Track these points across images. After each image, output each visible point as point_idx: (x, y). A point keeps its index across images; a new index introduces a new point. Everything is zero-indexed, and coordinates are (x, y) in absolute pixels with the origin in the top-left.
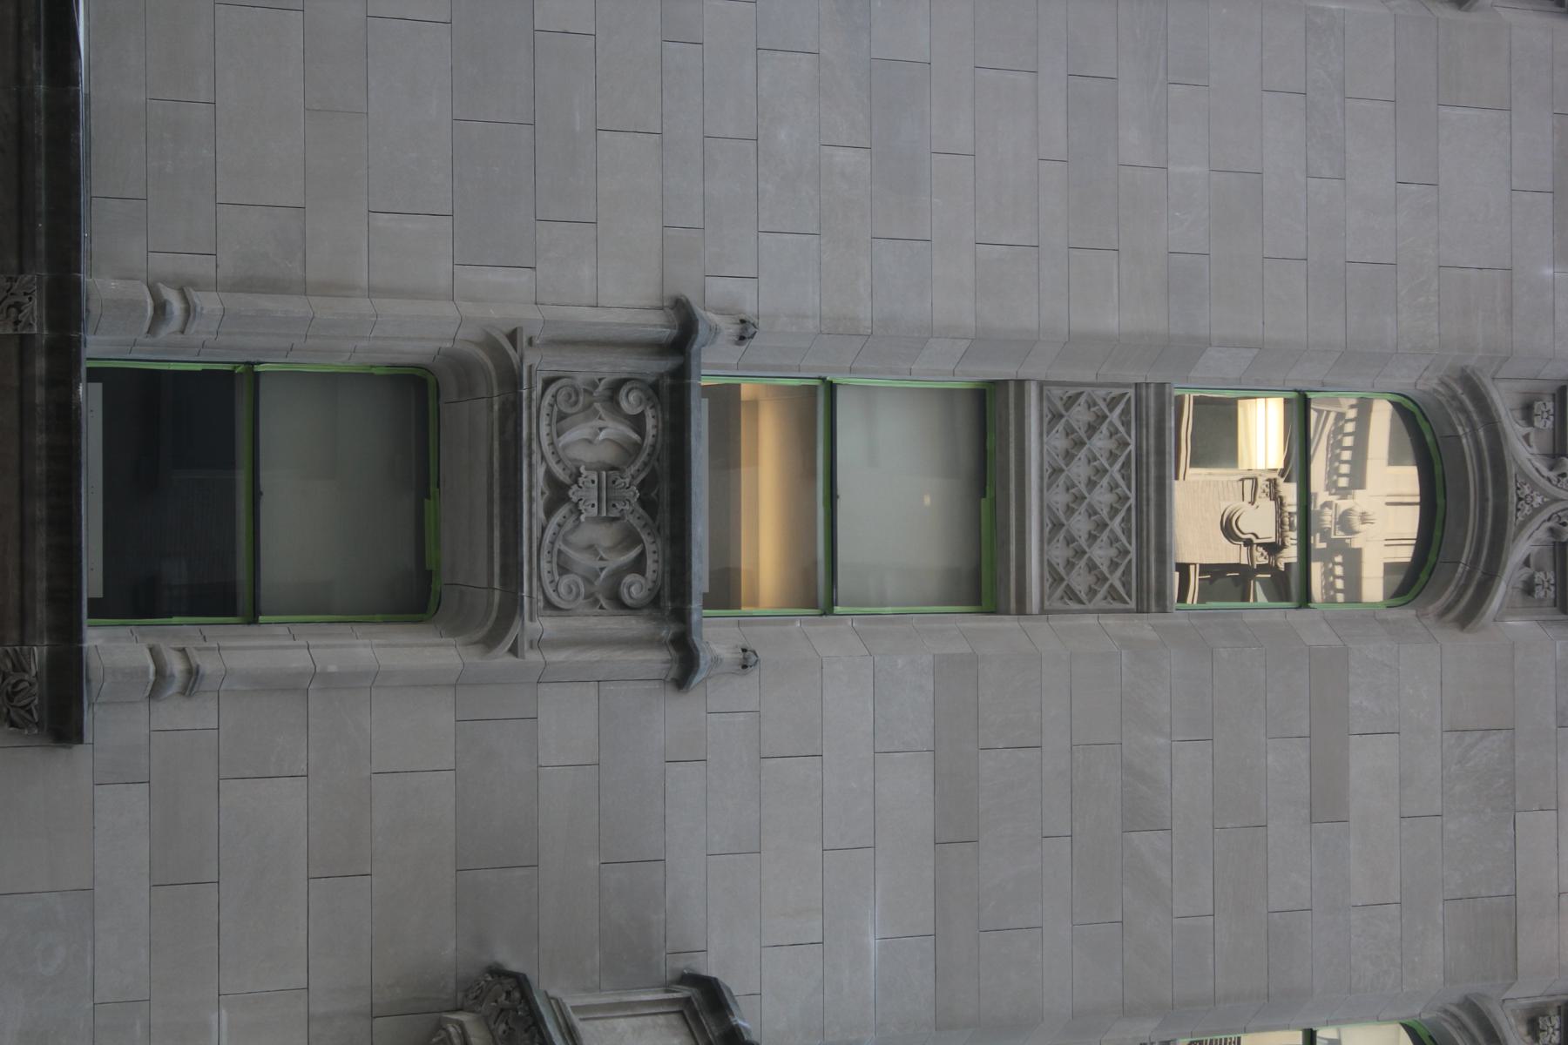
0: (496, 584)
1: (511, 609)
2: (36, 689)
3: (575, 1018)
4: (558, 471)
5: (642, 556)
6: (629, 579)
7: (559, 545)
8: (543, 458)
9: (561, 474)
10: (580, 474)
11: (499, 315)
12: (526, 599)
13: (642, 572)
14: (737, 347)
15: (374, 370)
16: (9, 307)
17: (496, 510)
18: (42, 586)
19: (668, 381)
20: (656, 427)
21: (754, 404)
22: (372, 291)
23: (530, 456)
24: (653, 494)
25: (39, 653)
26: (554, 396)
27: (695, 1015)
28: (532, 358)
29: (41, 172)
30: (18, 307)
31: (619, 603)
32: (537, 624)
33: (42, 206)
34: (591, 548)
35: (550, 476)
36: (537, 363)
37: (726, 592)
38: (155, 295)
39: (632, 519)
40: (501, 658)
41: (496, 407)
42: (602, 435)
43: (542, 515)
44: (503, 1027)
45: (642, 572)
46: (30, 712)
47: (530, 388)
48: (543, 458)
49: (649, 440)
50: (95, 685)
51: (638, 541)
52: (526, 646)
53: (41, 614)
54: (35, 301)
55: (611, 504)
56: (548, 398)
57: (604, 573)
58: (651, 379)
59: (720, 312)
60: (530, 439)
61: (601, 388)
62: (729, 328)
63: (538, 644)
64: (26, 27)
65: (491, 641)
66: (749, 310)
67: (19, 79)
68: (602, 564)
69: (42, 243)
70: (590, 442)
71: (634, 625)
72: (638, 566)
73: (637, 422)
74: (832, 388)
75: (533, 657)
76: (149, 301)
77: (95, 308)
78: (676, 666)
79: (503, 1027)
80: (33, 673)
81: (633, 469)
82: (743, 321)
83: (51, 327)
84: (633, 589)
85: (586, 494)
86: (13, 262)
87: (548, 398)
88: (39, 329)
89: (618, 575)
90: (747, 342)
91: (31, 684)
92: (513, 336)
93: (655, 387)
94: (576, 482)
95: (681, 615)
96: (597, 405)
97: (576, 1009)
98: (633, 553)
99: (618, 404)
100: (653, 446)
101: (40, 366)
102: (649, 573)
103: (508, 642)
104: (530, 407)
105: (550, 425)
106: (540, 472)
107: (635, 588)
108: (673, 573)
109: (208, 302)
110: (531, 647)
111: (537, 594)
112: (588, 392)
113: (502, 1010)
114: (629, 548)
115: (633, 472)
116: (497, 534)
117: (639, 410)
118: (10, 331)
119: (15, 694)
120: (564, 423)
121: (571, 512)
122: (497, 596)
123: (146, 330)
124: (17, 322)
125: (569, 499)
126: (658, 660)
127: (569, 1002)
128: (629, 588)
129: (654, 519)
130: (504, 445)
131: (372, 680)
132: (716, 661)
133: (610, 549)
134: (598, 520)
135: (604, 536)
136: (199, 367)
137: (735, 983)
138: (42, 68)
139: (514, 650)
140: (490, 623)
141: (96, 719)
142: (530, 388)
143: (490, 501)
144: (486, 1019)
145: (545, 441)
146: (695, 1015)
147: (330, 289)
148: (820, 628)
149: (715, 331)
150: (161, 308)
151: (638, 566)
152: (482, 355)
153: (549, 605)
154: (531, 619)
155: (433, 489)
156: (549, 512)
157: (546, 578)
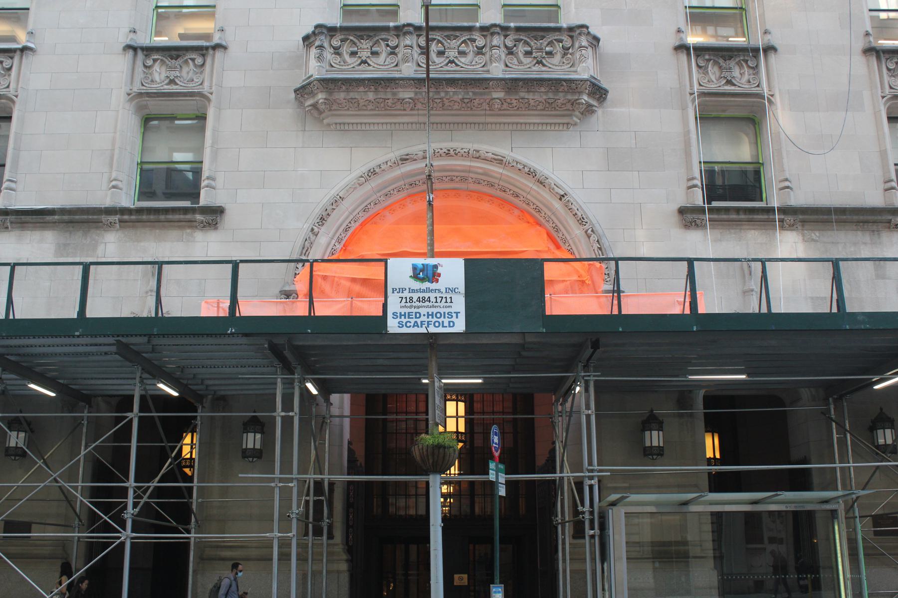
0: (194, 98)
1: (200, 94)
3: (308, 76)
4: (166, 82)
5: (191, 59)
6: (196, 62)
7: (185, 82)
8: (162, 86)
9: (167, 81)
11: (123, 97)
12: (199, 90)
13: (195, 59)
14: (138, 34)
15: (142, 131)
17: (175, 98)
18: (182, 217)
19: (145, 52)
20: (156, 55)
21: (185, 29)
22: (115, 132)
23: (161, 90)
24: (174, 56)
25: (199, 217)
26: (146, 83)
27: (310, 43)
28: (135, 90)
29: (77, 217)
30: (111, 223)
31: (203, 65)
32: (205, 87)
33: (85, 217)
34: (188, 73)
35: (168, 84)
36: (137, 88)
37: (207, 37)
38: (110, 189)
39: (182, 60)
40: (212, 97)
41: (148, 99)
42: (158, 70)
43: (177, 86)
44: (305, 96)
45: (195, 59)
47: (144, 90)
48: (162, 86)
49: (160, 57)
50: (209, 203)
51: (187, 60)
52: (211, 90)
53: (189, 217)
54: (109, 218)
55: (176, 67)
56: (147, 85)
57: (195, 69)
58: (144, 57)
59: (127, 38)
60: (157, 90)
61: (146, 71)
62: (132, 35)
63: (211, 87)
64: (42, 221)
65: (209, 100)
66: (128, 30)
67: (55, 222)
68: (192, 70)
69: (95, 217)
70: (160, 74)
71: (209, 60)
72: (193, 60)
73: (155, 61)
74: (157, 7)
75: (214, 88)
76: (113, 189)
77: (113, 203)
78: (220, 49)
79: (305, 96)
81: (167, 62)
82: (130, 32)
83: (117, 215)
84: (199, 61)
85: (172, 74)
86: (101, 224)
87: (147, 85)
88: (117, 218)
89: (195, 66)
90: (136, 30)
91: (206, 219)
92: (129, 94)
93: (146, 56)
95: (207, 48)
96: (150, 71)
97: (305, 76)
98: (190, 61)
99: (150, 66)
100: (162, 56)
101: (126, 217)
102: (195, 57)
103: (209, 95)
104: (148, 90)
105: (153, 84)
106: (166, 87)
107: (199, 61)
108: (196, 50)
109: (114, 175)
110: (211, 89)
112: (147, 74)
113: (302, 96)
114: (189, 63)
115: (169, 62)
116: (180, 98)
117: (152, 60)
118: (118, 225)
119: (209, 223)
120: (154, 81)
121: (177, 78)
122: (197, 98)
123: (120, 191)
124: (115, 223)
126: (219, 54)
127: (304, 78)
128: (198, 62)
130: (158, 97)
131: (214, 130)
132: (220, 38)
133: (189, 67)
134: (181, 71)
135: (185, 69)
136: (138, 177)
137: (304, 34)
138: (52, 217)
139: (211, 94)
140: (204, 100)
141: (218, 202)
142: (144, 90)
143: (172, 100)
144: (305, 100)
145: (158, 85)
146: (310, 43)
147: (113, 144)
148: (219, 11)
149: (132, 39)
150: (114, 187)
151: (193, 60)
152: (134, 103)
153: (201, 84)
154: (204, 89)
155: (174, 116)
156: (176, 84)
157: (194, 85)
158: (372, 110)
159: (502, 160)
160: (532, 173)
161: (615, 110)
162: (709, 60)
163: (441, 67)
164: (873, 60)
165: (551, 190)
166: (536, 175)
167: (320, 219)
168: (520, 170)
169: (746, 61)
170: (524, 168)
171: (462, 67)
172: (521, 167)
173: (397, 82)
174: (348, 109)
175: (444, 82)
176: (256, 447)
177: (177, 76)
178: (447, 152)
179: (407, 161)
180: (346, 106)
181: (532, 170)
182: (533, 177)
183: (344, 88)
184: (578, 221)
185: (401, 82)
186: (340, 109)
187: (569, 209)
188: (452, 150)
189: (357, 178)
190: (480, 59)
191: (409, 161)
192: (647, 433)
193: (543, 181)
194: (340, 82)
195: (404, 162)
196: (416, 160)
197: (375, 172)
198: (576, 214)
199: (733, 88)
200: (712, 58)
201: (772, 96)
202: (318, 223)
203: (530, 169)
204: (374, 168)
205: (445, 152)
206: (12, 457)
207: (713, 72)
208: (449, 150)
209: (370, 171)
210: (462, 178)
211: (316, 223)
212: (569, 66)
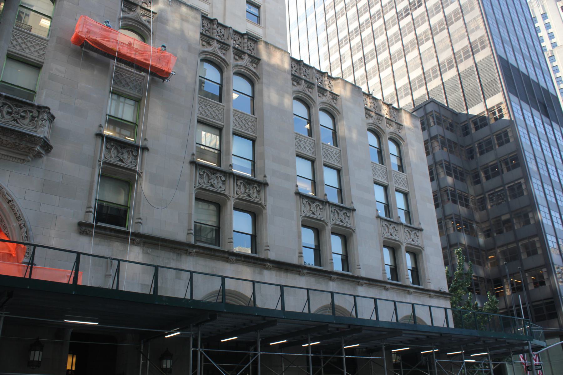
161: (54, 159)
162: (113, 146)
164: (298, 197)
169: (132, 152)
192: (165, 361)
199: (122, 164)
200: (115, 145)
201: (141, 173)
207: (114, 152)
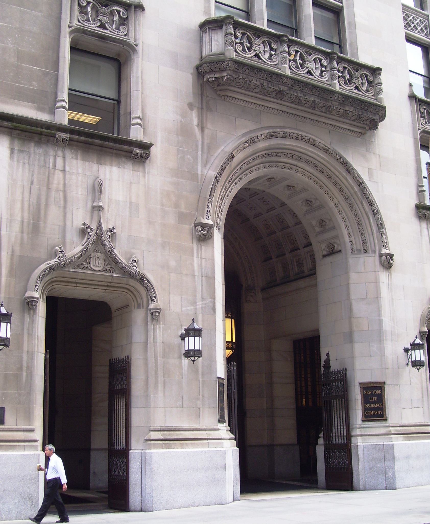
2: (142, 152)
9: (99, 24)
10: (99, 20)
16: (62, 141)
30: (63, 139)
35: (99, 27)
46: (147, 154)
48: (95, 27)
80: (139, 151)
81: (98, 7)
94: (101, 21)
101: (76, 137)
103: (135, 46)
111: (122, 36)
125: (105, 24)
129: (109, 5)
158: (255, 92)
159: (328, 150)
160: (345, 164)
163: (304, 74)
165: (354, 178)
166: (347, 166)
167: (221, 170)
168: (337, 160)
170: (340, 159)
171: (315, 77)
172: (339, 158)
173: (282, 78)
174: (241, 88)
175: (309, 86)
176: (196, 349)
177: (108, 22)
178: (297, 136)
179: (272, 137)
180: (241, 85)
181: (345, 161)
182: (345, 167)
183: (247, 71)
184: (369, 202)
185: (284, 78)
186: (236, 86)
187: (364, 194)
188: (300, 136)
189: (243, 143)
190: (326, 75)
191: (274, 137)
193: (350, 171)
194: (246, 67)
195: (271, 137)
196: (278, 138)
197: (254, 141)
198: (368, 198)
202: (220, 172)
203: (344, 160)
204: (254, 138)
205: (296, 136)
206: (191, 358)
208: (298, 135)
209: (251, 139)
210: (299, 157)
211: (219, 172)
212: (372, 95)
